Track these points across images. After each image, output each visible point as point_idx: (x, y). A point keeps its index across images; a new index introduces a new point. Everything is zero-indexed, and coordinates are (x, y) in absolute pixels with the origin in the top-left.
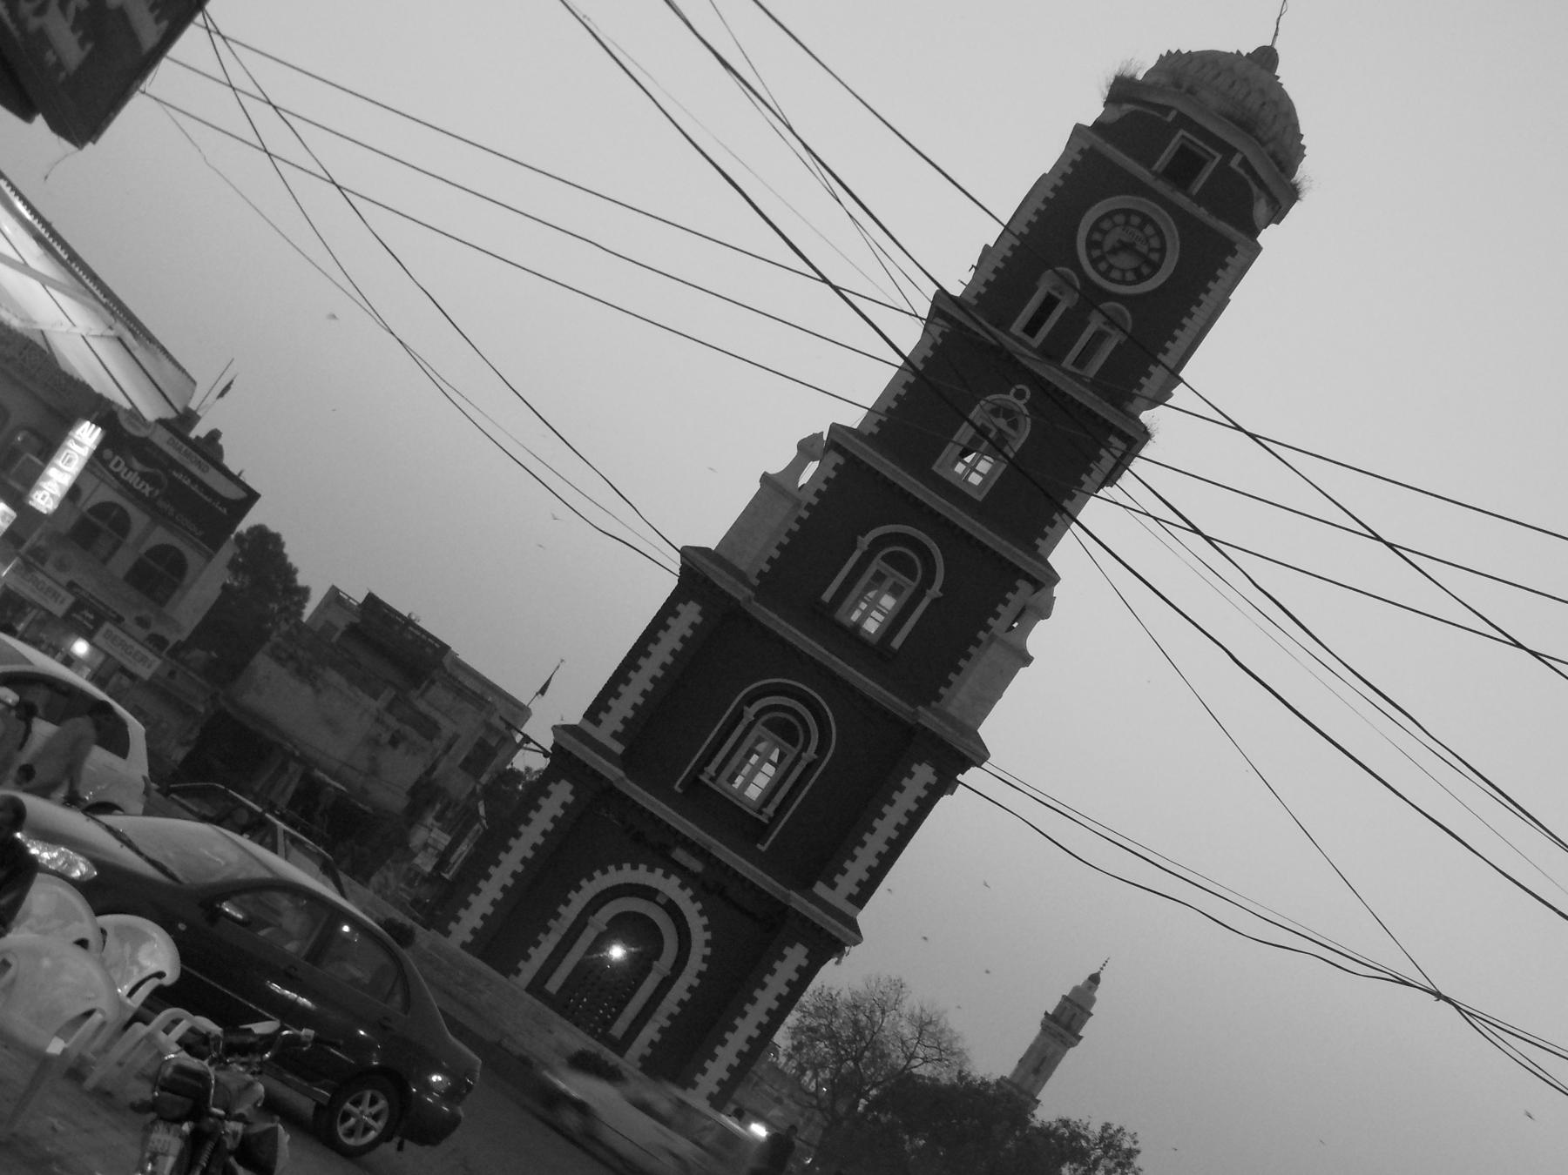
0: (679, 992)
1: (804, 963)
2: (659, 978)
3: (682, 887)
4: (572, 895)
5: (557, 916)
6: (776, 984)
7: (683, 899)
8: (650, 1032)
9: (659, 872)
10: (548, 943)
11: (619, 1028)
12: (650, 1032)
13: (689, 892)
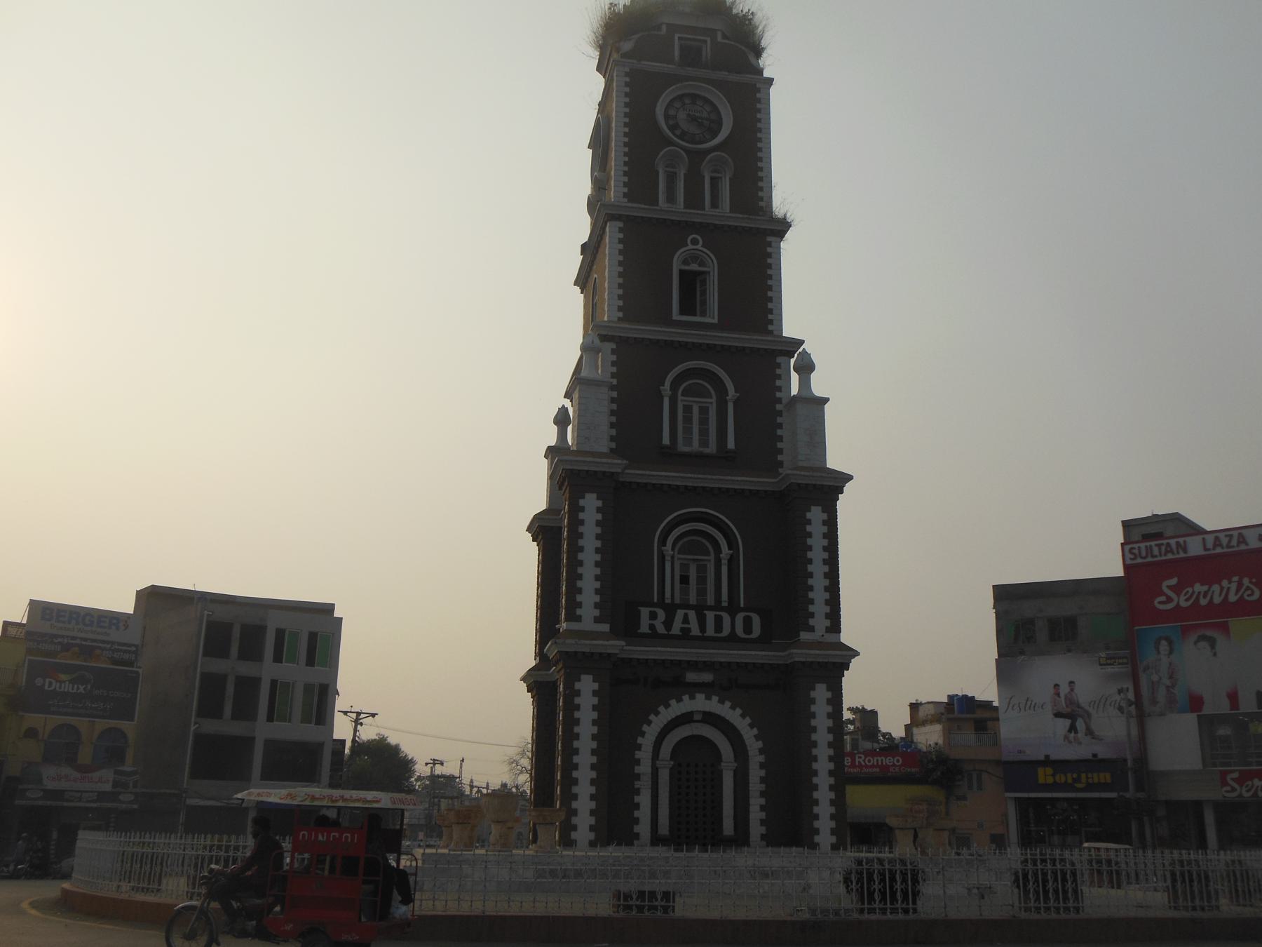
0: (756, 774)
1: (829, 695)
2: (731, 773)
3: (708, 698)
4: (638, 755)
5: (638, 777)
6: (822, 722)
7: (713, 705)
8: (756, 814)
9: (686, 698)
10: (644, 799)
11: (728, 827)
12: (756, 814)
13: (715, 699)
